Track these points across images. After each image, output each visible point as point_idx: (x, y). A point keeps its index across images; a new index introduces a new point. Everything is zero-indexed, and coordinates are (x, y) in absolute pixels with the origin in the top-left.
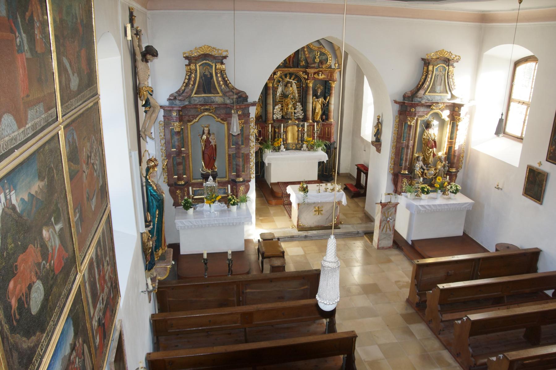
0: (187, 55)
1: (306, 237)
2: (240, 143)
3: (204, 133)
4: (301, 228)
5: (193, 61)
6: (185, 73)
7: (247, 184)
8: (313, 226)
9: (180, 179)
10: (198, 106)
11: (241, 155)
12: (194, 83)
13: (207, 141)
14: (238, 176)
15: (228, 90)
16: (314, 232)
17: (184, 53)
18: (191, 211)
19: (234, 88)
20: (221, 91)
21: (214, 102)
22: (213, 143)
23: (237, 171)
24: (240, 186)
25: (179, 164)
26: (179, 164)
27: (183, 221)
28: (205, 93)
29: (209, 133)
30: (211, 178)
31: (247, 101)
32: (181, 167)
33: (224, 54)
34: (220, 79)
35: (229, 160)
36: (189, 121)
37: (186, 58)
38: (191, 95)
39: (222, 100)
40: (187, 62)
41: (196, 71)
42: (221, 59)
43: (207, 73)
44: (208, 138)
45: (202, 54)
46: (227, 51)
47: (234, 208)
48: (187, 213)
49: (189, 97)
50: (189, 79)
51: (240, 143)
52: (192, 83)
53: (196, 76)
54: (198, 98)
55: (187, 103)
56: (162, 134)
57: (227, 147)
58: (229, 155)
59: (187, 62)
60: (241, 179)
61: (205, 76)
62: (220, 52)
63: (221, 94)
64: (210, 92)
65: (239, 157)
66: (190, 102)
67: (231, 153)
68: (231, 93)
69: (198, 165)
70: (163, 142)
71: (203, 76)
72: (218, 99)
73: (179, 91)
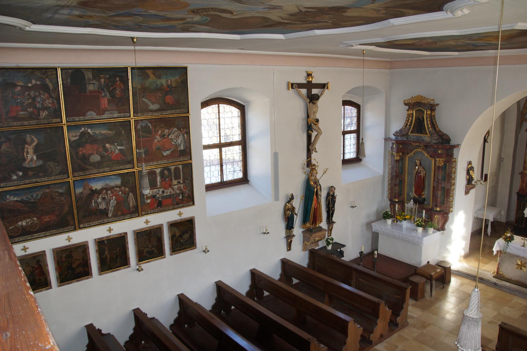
0: (406, 102)
1: (495, 284)
2: (440, 178)
3: (417, 166)
4: (498, 276)
5: (411, 107)
6: (406, 116)
7: (445, 215)
8: (514, 279)
9: (395, 198)
10: (412, 143)
11: (440, 188)
12: (411, 124)
13: (418, 173)
14: (436, 206)
15: (434, 132)
16: (508, 284)
17: (405, 101)
18: (389, 221)
19: (440, 131)
20: (429, 132)
21: (423, 141)
22: (422, 174)
23: (436, 201)
24: (435, 214)
25: (396, 185)
26: (396, 185)
27: (377, 225)
28: (418, 133)
29: (421, 164)
30: (412, 200)
31: (449, 143)
32: (397, 188)
33: (432, 102)
34: (429, 123)
35: (433, 191)
36: (408, 154)
37: (406, 104)
38: (408, 133)
39: (430, 139)
40: (407, 107)
41: (413, 114)
42: (432, 107)
43: (420, 117)
44: (419, 169)
45: (416, 102)
46: (433, 100)
47: (420, 229)
48: (386, 222)
49: (407, 135)
50: (408, 121)
51: (440, 178)
52: (409, 124)
53: (412, 118)
54: (413, 136)
55: (405, 139)
56: (390, 161)
57: (432, 179)
58: (434, 187)
59: (407, 107)
60: (438, 209)
61: (419, 119)
62: (429, 100)
63: (429, 135)
64: (421, 133)
65: (438, 190)
66: (407, 139)
67: (435, 185)
68: (436, 135)
69: (409, 190)
70: (390, 166)
71: (417, 119)
72: (426, 138)
73: (401, 129)
